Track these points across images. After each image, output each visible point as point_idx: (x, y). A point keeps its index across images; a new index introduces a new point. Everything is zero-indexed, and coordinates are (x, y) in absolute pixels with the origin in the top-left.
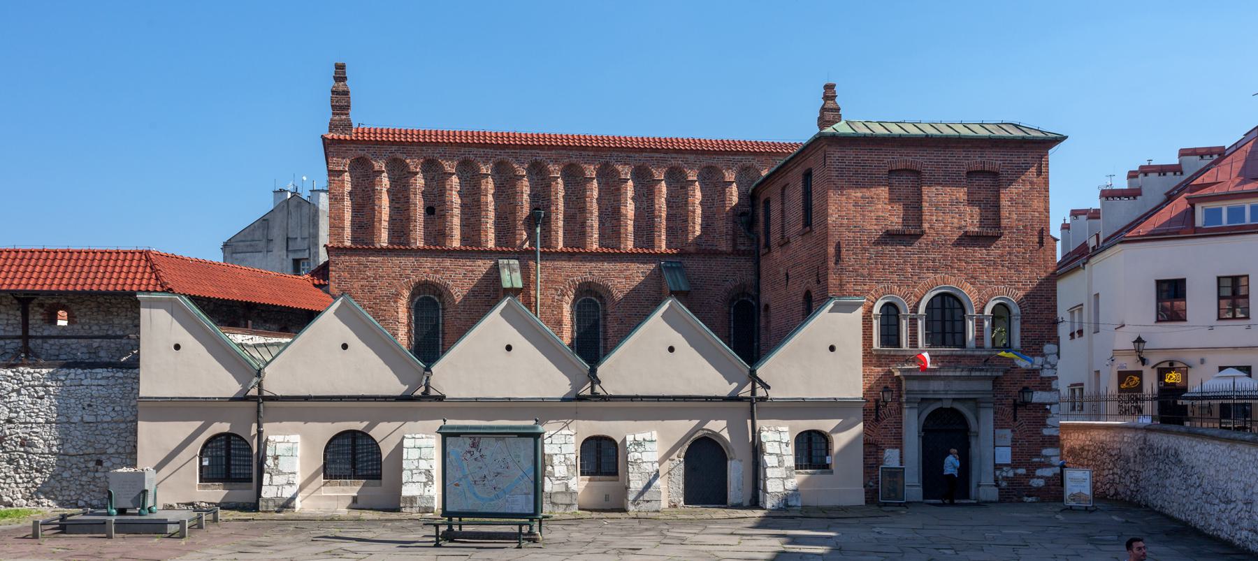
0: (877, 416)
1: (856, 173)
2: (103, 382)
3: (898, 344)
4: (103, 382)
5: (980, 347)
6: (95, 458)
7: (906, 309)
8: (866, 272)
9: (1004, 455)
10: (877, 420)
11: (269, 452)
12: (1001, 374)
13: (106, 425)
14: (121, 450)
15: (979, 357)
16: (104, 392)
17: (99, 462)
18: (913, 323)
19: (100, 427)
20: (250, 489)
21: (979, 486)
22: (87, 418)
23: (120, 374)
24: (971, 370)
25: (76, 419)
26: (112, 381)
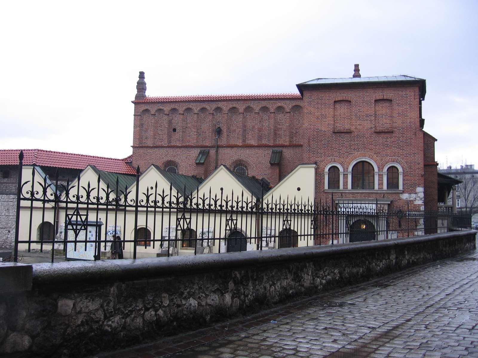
1: (318, 103)
3: (339, 187)
5: (380, 188)
6: (8, 229)
7: (341, 169)
8: (322, 151)
12: (389, 203)
15: (381, 193)
17: (9, 232)
18: (345, 176)
22: (7, 214)
25: (3, 214)
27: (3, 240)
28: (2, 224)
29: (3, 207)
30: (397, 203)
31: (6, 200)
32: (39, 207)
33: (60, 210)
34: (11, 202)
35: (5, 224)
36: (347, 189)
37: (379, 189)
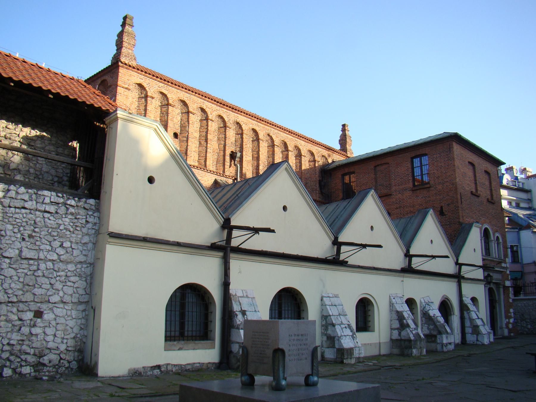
2: (52, 209)
4: (52, 209)
11: (236, 308)
13: (50, 264)
14: (67, 299)
16: (52, 222)
17: (39, 314)
19: (43, 266)
20: (214, 348)
22: (26, 253)
23: (72, 202)
25: (12, 253)
26: (62, 210)
27: (7, 348)
28: (6, 286)
29: (10, 227)
31: (27, 205)
32: (172, 239)
33: (232, 255)
34: (47, 215)
35: (20, 286)
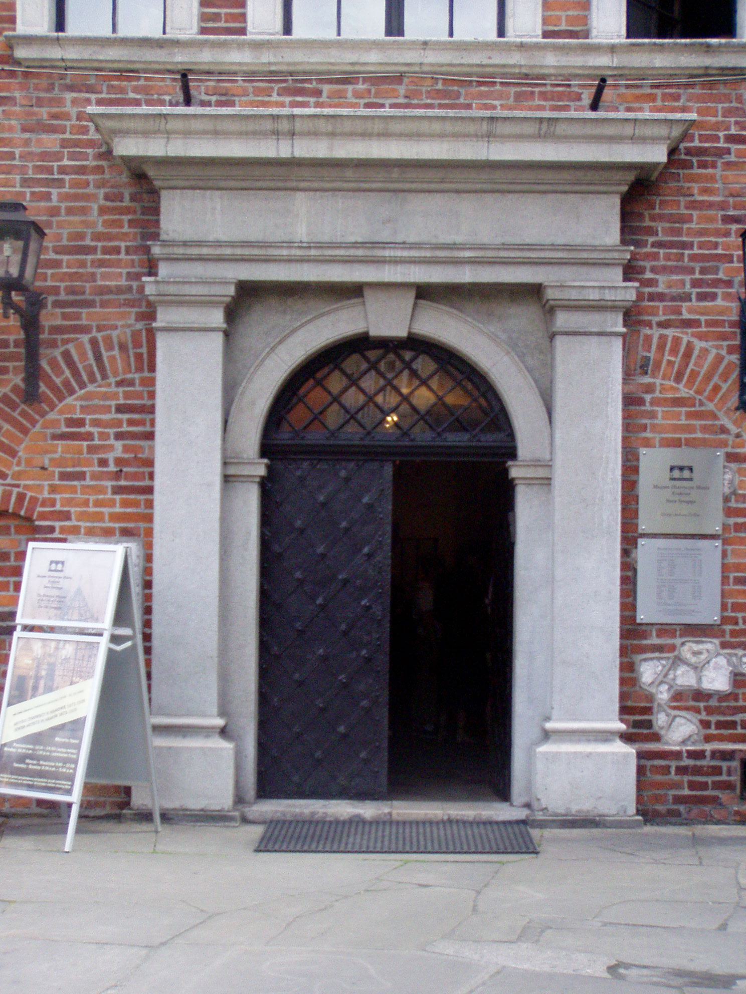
0: (33, 374)
9: (688, 583)
10: (30, 395)
12: (658, 154)
21: (546, 735)
24: (491, 129)
30: (718, 172)
36: (243, 31)
37: (546, 34)
